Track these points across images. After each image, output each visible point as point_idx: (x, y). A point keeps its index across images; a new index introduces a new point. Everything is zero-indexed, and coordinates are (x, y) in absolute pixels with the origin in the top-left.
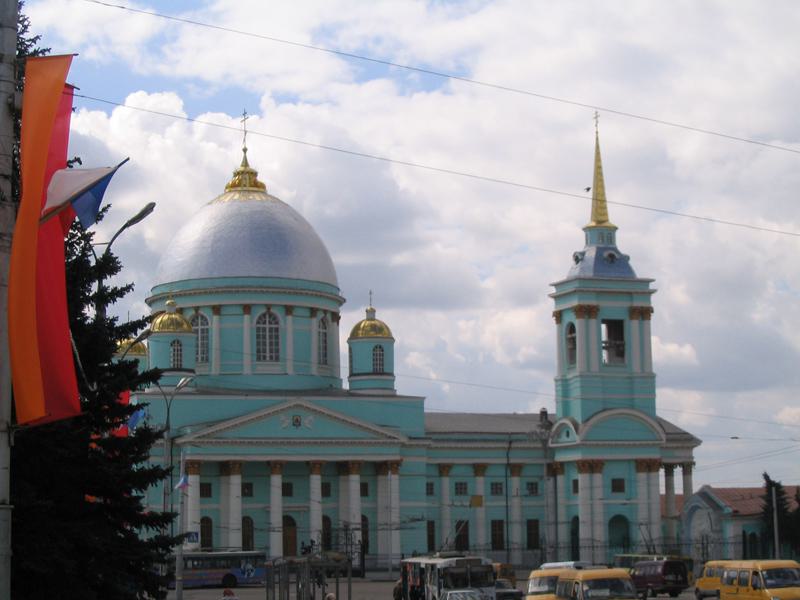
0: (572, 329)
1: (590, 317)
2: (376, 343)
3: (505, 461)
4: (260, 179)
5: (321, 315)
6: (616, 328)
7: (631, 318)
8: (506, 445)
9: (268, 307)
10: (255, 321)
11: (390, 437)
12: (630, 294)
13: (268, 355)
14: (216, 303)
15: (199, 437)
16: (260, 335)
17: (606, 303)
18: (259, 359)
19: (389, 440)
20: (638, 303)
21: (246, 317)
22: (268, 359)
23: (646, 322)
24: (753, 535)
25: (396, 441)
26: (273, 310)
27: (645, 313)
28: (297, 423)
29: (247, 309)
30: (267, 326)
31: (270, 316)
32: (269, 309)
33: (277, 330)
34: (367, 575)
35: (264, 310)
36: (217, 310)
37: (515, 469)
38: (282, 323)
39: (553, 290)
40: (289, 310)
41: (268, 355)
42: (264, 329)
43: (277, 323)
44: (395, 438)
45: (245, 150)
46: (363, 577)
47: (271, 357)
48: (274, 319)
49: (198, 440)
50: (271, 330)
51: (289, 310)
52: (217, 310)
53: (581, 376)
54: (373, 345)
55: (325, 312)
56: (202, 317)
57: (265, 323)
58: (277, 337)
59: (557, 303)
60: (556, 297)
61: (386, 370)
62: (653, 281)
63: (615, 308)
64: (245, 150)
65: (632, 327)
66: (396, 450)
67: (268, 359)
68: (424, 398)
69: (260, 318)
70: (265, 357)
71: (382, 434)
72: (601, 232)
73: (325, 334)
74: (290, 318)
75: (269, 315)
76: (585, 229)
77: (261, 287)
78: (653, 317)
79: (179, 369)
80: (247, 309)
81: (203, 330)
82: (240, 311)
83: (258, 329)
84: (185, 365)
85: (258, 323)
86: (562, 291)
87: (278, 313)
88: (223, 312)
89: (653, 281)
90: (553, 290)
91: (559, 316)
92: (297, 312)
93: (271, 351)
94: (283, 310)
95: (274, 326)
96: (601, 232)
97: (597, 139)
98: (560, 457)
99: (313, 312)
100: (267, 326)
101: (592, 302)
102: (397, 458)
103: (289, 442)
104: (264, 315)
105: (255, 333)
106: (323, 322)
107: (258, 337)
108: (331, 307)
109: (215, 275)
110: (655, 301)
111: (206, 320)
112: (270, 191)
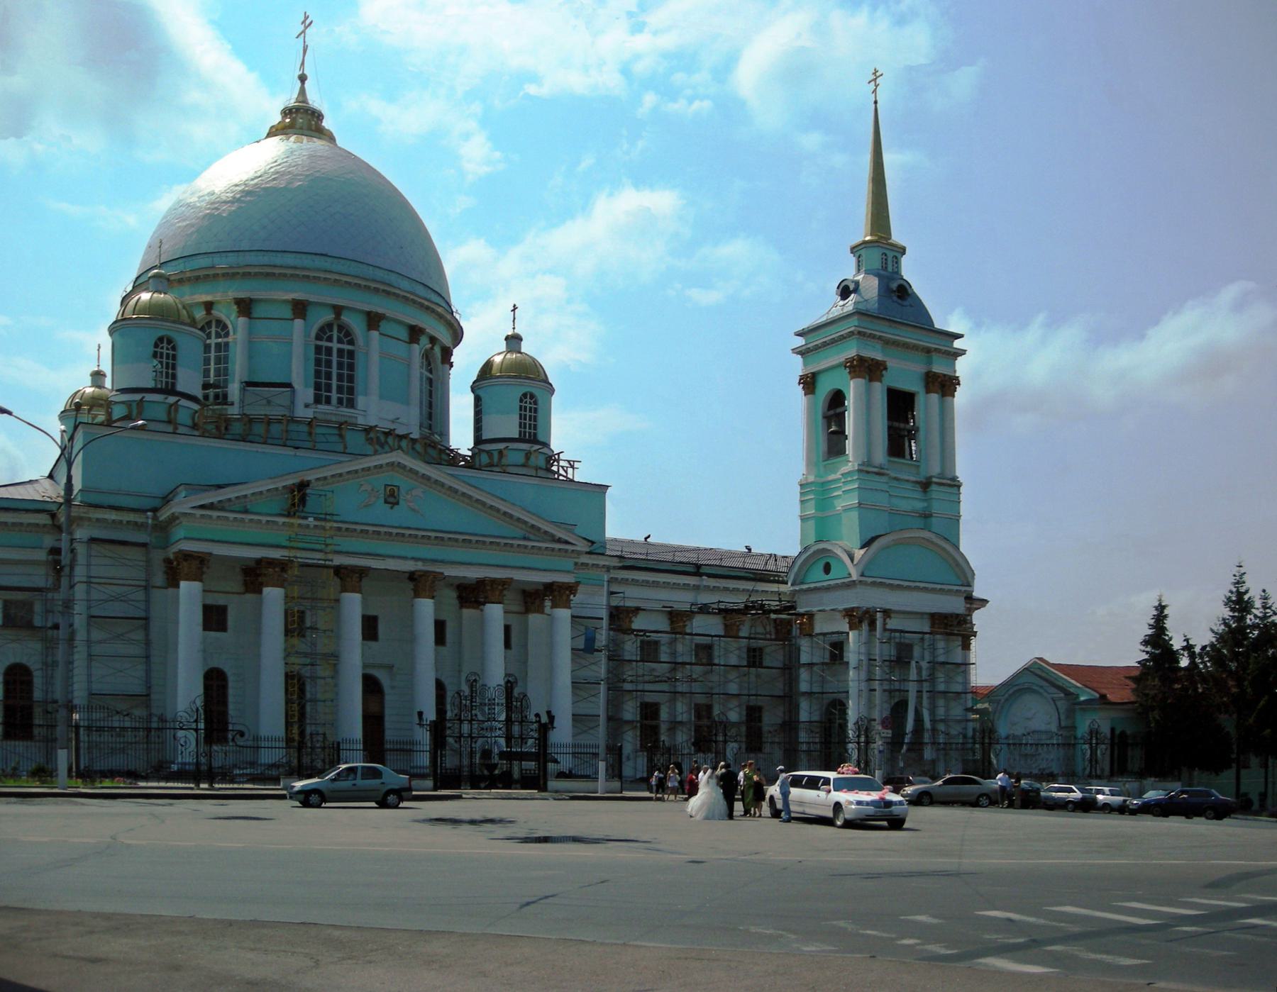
0: (837, 399)
1: (871, 380)
2: (520, 387)
5: (424, 341)
6: (900, 404)
7: (928, 391)
9: (338, 310)
10: (313, 334)
11: (560, 541)
12: (928, 351)
13: (334, 395)
14: (242, 295)
15: (202, 507)
16: (321, 358)
17: (884, 372)
18: (317, 400)
19: (557, 546)
20: (939, 368)
21: (298, 323)
22: (334, 401)
23: (949, 398)
24: (1123, 734)
25: (570, 548)
26: (346, 318)
27: (946, 385)
28: (392, 498)
29: (300, 309)
30: (335, 346)
31: (341, 328)
33: (351, 354)
35: (329, 316)
38: (360, 341)
39: (800, 341)
40: (373, 320)
41: (334, 395)
42: (329, 350)
43: (351, 342)
44: (567, 542)
46: (543, 788)
47: (340, 401)
48: (347, 335)
49: (199, 512)
50: (340, 352)
52: (245, 307)
53: (860, 471)
55: (433, 340)
56: (219, 322)
58: (351, 367)
59: (805, 364)
60: (803, 352)
61: (541, 438)
65: (926, 405)
66: (568, 564)
67: (334, 401)
68: (603, 488)
69: (322, 330)
70: (328, 401)
71: (546, 532)
72: (881, 250)
73: (430, 381)
74: (375, 334)
76: (853, 250)
78: (960, 391)
79: (170, 390)
80: (300, 309)
81: (218, 346)
83: (318, 349)
84: (179, 388)
85: (318, 338)
86: (814, 341)
87: (356, 324)
88: (258, 311)
89: (960, 336)
90: (800, 341)
91: (809, 383)
92: (384, 326)
93: (340, 389)
99: (415, 333)
101: (874, 352)
104: (329, 326)
105: (312, 355)
106: (427, 356)
107: (318, 362)
109: (245, 246)
110: (962, 367)
111: (225, 327)
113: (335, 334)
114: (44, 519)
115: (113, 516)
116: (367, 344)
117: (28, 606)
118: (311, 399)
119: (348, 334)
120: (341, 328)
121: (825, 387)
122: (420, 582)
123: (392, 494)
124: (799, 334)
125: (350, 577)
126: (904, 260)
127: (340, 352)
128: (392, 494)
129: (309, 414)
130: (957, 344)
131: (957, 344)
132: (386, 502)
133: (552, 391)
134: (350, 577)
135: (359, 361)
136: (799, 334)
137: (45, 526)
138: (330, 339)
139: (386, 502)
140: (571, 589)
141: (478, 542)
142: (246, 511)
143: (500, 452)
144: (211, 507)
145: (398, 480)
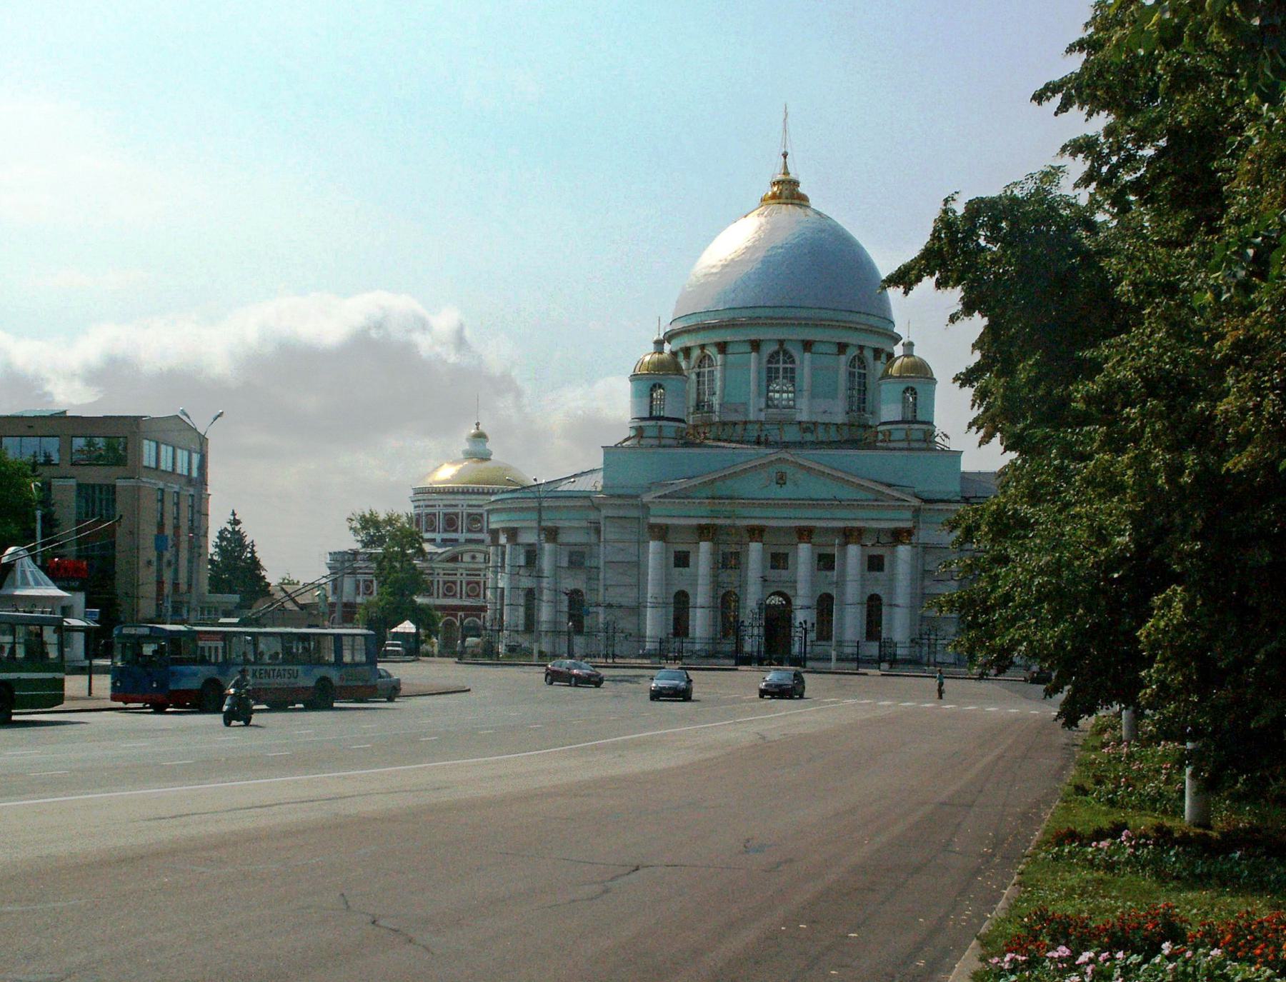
4: (802, 189)
9: (781, 342)
10: (765, 360)
11: (898, 499)
26: (788, 347)
29: (756, 345)
30: (781, 366)
33: (793, 370)
34: (809, 664)
35: (776, 347)
37: (552, 534)
38: (797, 362)
40: (807, 345)
42: (777, 369)
43: (793, 362)
45: (785, 155)
50: (785, 369)
51: (807, 345)
52: (722, 347)
54: (903, 387)
55: (861, 348)
57: (778, 362)
64: (785, 155)
74: (807, 355)
77: (772, 318)
80: (756, 345)
82: (747, 348)
83: (769, 370)
85: (769, 362)
87: (796, 352)
88: (730, 349)
94: (800, 346)
95: (788, 366)
99: (842, 348)
100: (781, 366)
102: (909, 525)
103: (767, 503)
104: (777, 353)
108: (872, 342)
112: (814, 203)
114: (587, 503)
115: (619, 502)
116: (802, 362)
117: (582, 555)
118: (763, 406)
119: (791, 356)
120: (786, 353)
122: (805, 534)
123: (781, 478)
125: (756, 533)
127: (785, 369)
128: (781, 478)
129: (762, 417)
133: (932, 381)
134: (756, 533)
135: (798, 371)
140: (909, 532)
141: (838, 503)
142: (688, 497)
143: (889, 431)
144: (665, 496)
145: (784, 468)
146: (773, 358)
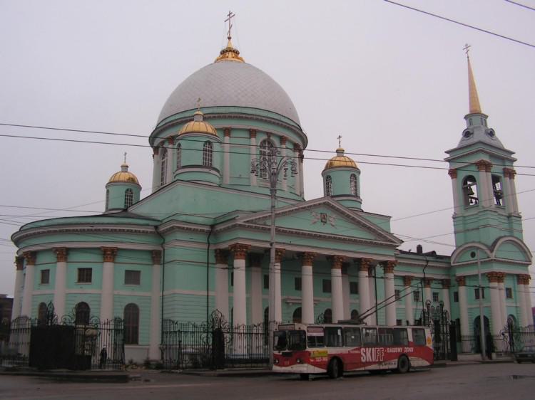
3: (422, 276)
8: (424, 263)
9: (269, 134)
15: (248, 222)
19: (389, 243)
23: (512, 180)
26: (272, 138)
31: (269, 143)
32: (269, 137)
35: (265, 137)
36: (227, 131)
39: (448, 156)
40: (283, 140)
44: (392, 242)
48: (271, 145)
51: (283, 140)
62: (514, 153)
63: (497, 169)
72: (475, 116)
75: (267, 143)
79: (211, 167)
80: (253, 133)
82: (246, 135)
86: (454, 156)
87: (276, 141)
88: (233, 134)
89: (514, 153)
90: (448, 156)
91: (453, 173)
96: (475, 116)
97: (468, 60)
98: (460, 273)
101: (486, 158)
104: (264, 141)
113: (267, 145)
121: (462, 175)
124: (447, 152)
126: (488, 120)
130: (513, 156)
131: (513, 156)
132: (322, 221)
136: (447, 152)
137: (151, 232)
138: (265, 147)
139: (322, 221)
146: (262, 145)
